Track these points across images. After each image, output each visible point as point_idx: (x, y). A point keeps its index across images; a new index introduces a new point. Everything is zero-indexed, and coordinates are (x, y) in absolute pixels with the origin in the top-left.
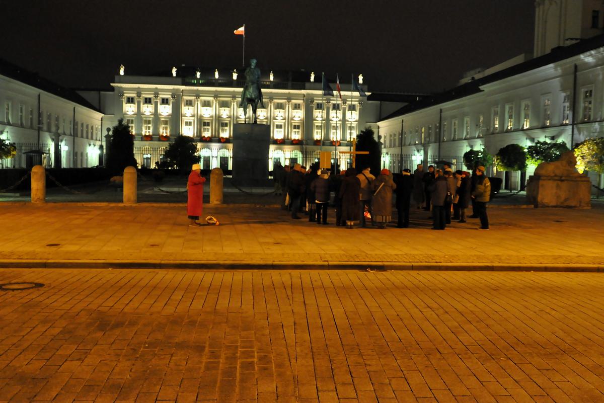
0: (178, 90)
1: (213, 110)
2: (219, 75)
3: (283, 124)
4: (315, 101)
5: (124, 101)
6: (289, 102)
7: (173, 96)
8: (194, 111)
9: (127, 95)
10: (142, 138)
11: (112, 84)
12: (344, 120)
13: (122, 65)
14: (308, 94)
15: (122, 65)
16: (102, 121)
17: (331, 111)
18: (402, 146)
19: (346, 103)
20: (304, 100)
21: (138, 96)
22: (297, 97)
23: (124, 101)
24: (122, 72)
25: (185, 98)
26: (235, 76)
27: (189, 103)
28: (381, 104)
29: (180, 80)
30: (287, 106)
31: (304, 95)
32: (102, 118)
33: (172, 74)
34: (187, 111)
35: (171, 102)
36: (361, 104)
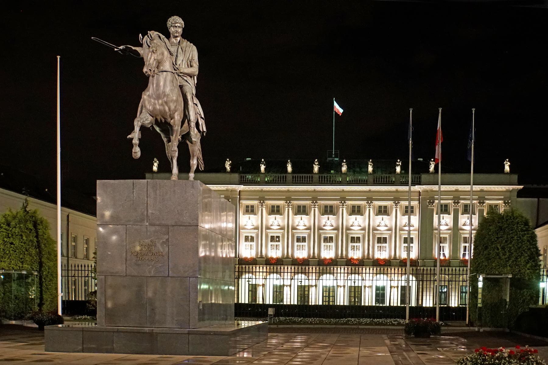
0: (232, 191)
1: (284, 218)
2: (292, 168)
6: (396, 204)
8: (257, 220)
17: (460, 216)
19: (483, 203)
22: (409, 196)
25: (245, 202)
28: (538, 200)
29: (236, 176)
30: (394, 209)
31: (420, 192)
36: (508, 203)
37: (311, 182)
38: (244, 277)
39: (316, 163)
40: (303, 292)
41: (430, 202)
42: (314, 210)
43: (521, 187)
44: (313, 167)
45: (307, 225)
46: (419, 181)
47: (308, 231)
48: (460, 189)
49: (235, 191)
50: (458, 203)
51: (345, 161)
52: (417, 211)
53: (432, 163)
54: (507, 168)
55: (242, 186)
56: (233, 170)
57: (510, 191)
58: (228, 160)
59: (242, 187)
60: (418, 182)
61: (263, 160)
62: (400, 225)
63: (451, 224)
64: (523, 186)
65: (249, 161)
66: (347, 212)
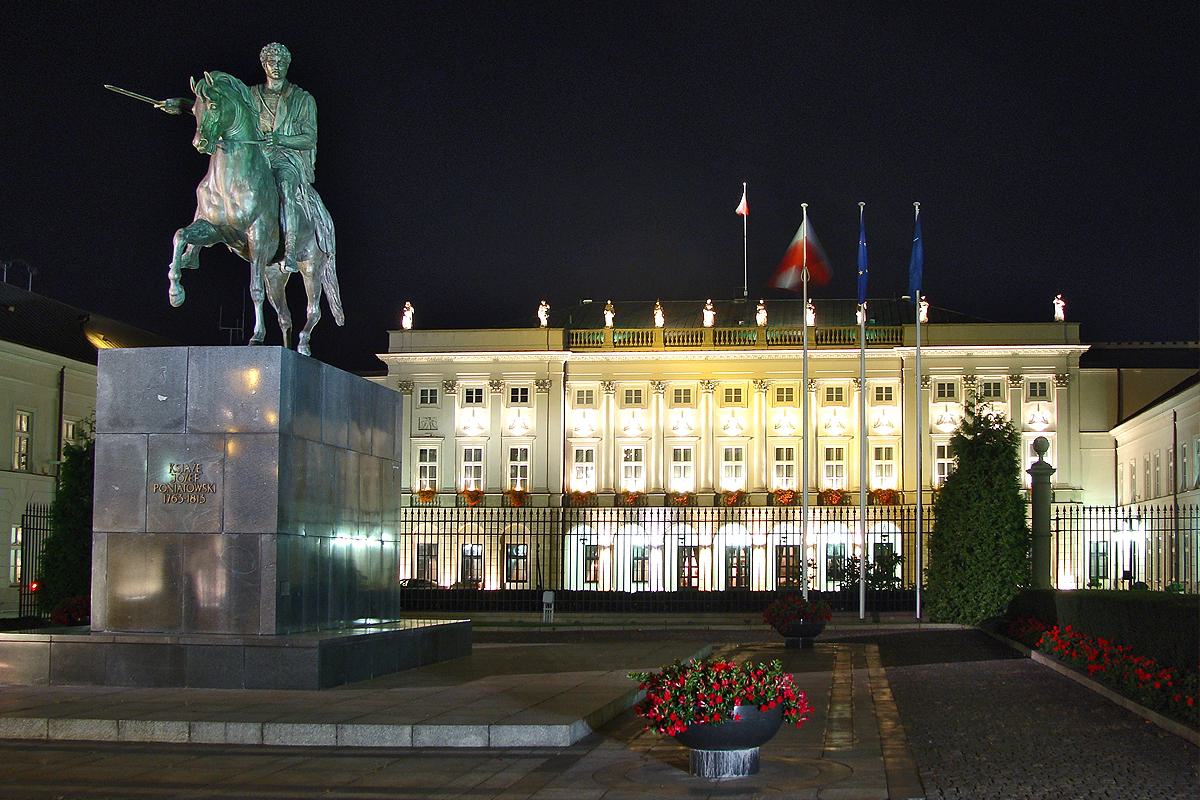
15: (408, 304)
18: (1176, 493)
19: (1019, 378)
24: (407, 322)
27: (586, 399)
28: (1119, 372)
29: (557, 335)
37: (699, 343)
39: (709, 307)
40: (688, 553)
43: (1087, 347)
46: (901, 339)
49: (557, 362)
51: (761, 302)
52: (897, 394)
53: (922, 304)
54: (1059, 313)
55: (570, 353)
56: (552, 324)
58: (544, 303)
59: (568, 356)
60: (899, 341)
61: (609, 302)
64: (1088, 347)
65: (587, 304)
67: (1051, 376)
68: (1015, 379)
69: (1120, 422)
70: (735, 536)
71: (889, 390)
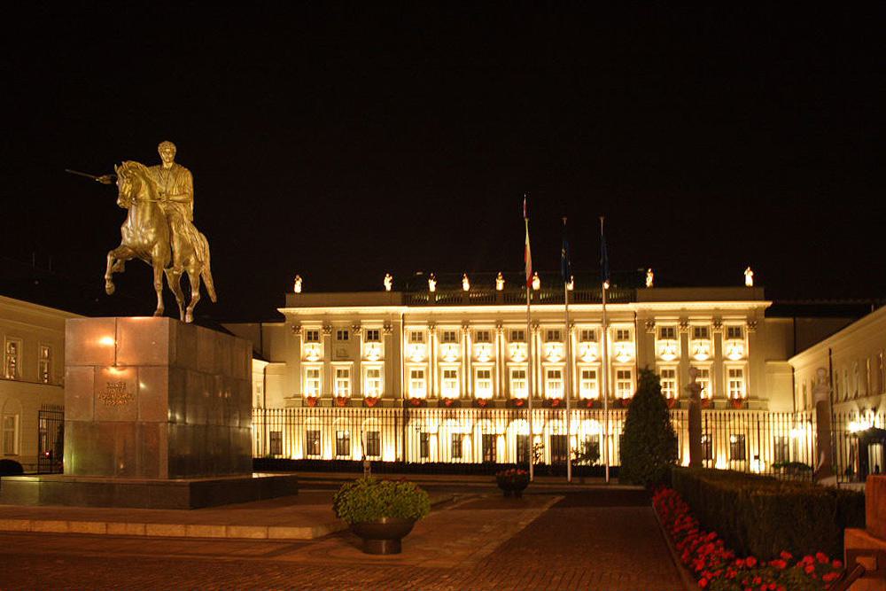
1: (461, 348)
3: (596, 370)
4: (657, 324)
5: (302, 338)
7: (387, 326)
9: (308, 326)
10: (333, 402)
11: (279, 309)
12: (719, 358)
13: (298, 277)
14: (644, 312)
15: (298, 277)
16: (265, 373)
19: (720, 325)
20: (635, 321)
21: (324, 328)
22: (620, 316)
23: (302, 338)
24: (298, 288)
26: (500, 285)
27: (418, 337)
29: (398, 295)
31: (635, 313)
32: (265, 369)
33: (385, 287)
34: (413, 353)
35: (383, 336)
38: (410, 423)
40: (489, 442)
41: (649, 325)
42: (500, 337)
43: (769, 304)
44: (496, 283)
45: (491, 356)
47: (492, 364)
48: (688, 308)
50: (686, 325)
54: (749, 281)
57: (756, 310)
62: (613, 354)
63: (679, 353)
66: (542, 339)
67: (744, 323)
68: (717, 322)
69: (795, 353)
70: (520, 427)
71: (627, 332)
